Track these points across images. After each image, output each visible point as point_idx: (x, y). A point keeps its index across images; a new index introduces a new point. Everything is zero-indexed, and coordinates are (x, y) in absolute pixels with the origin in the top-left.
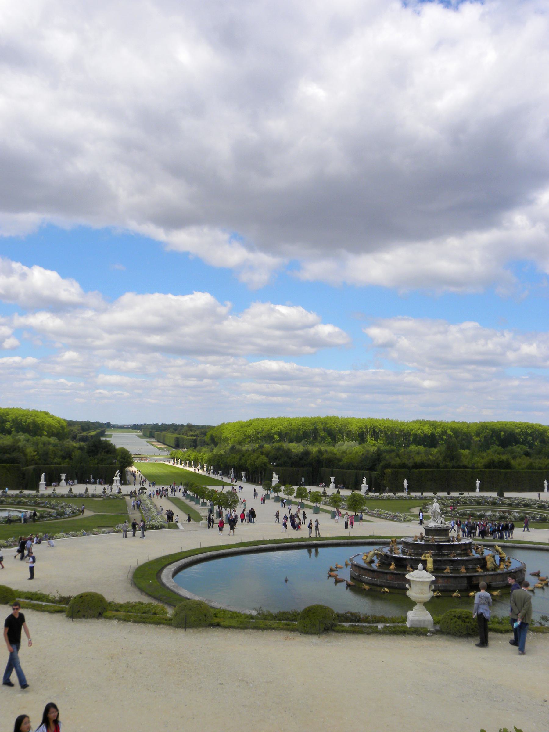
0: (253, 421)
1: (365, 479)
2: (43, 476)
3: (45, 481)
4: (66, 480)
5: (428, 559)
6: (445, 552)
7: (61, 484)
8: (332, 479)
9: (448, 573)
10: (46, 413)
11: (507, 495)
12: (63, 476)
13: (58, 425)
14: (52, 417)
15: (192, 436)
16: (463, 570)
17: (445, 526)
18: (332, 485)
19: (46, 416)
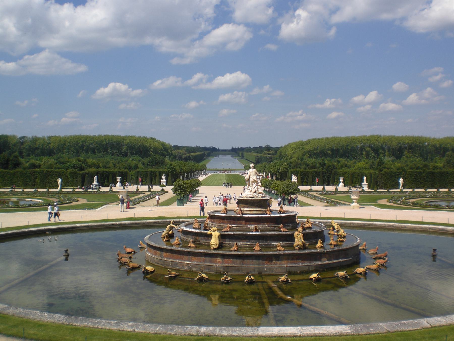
0: (311, 140)
1: (365, 178)
2: (96, 177)
3: (98, 181)
4: (123, 183)
5: (213, 233)
6: (252, 226)
8: (341, 180)
9: (235, 250)
10: (153, 139)
12: (119, 179)
13: (160, 147)
14: (158, 142)
15: (268, 154)
16: (257, 248)
18: (341, 184)
19: (152, 141)
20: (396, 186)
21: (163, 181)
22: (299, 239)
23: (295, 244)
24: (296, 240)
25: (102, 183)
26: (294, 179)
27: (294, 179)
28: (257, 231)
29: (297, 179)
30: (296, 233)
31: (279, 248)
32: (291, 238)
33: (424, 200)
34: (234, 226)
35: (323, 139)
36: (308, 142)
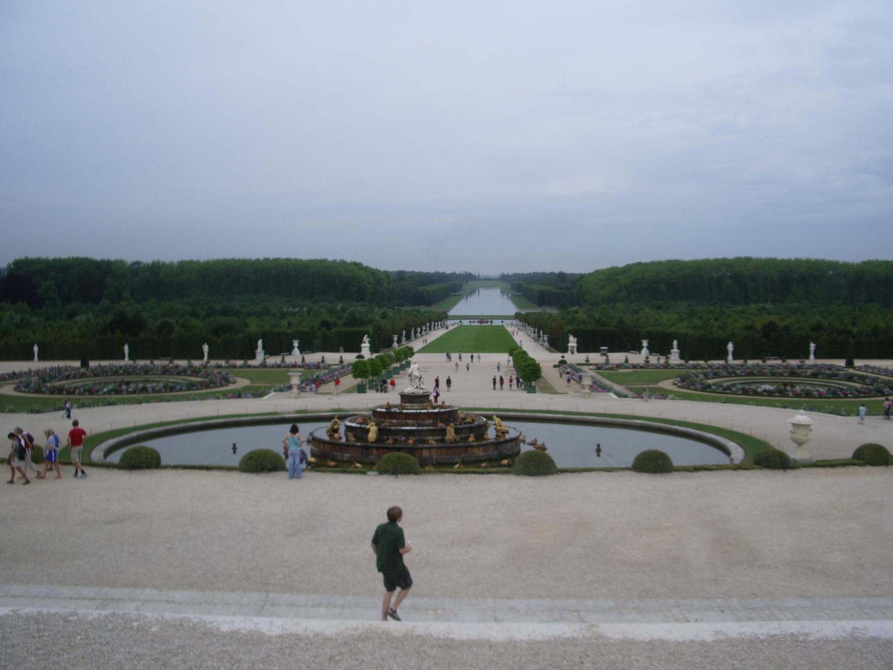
1: (675, 342)
2: (260, 343)
4: (302, 349)
6: (410, 422)
7: (293, 352)
10: (358, 265)
11: (858, 363)
12: (296, 344)
15: (561, 288)
16: (411, 442)
17: (421, 391)
20: (723, 355)
21: (366, 346)
22: (450, 434)
23: (447, 438)
24: (448, 434)
25: (270, 351)
26: (573, 342)
27: (573, 342)
28: (413, 426)
29: (578, 342)
30: (448, 428)
31: (432, 441)
32: (443, 432)
33: (726, 381)
34: (394, 421)
35: (652, 263)
36: (628, 268)
